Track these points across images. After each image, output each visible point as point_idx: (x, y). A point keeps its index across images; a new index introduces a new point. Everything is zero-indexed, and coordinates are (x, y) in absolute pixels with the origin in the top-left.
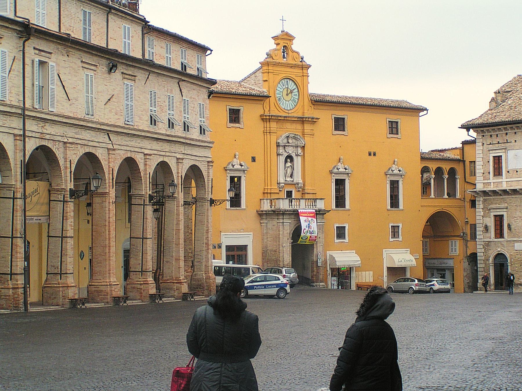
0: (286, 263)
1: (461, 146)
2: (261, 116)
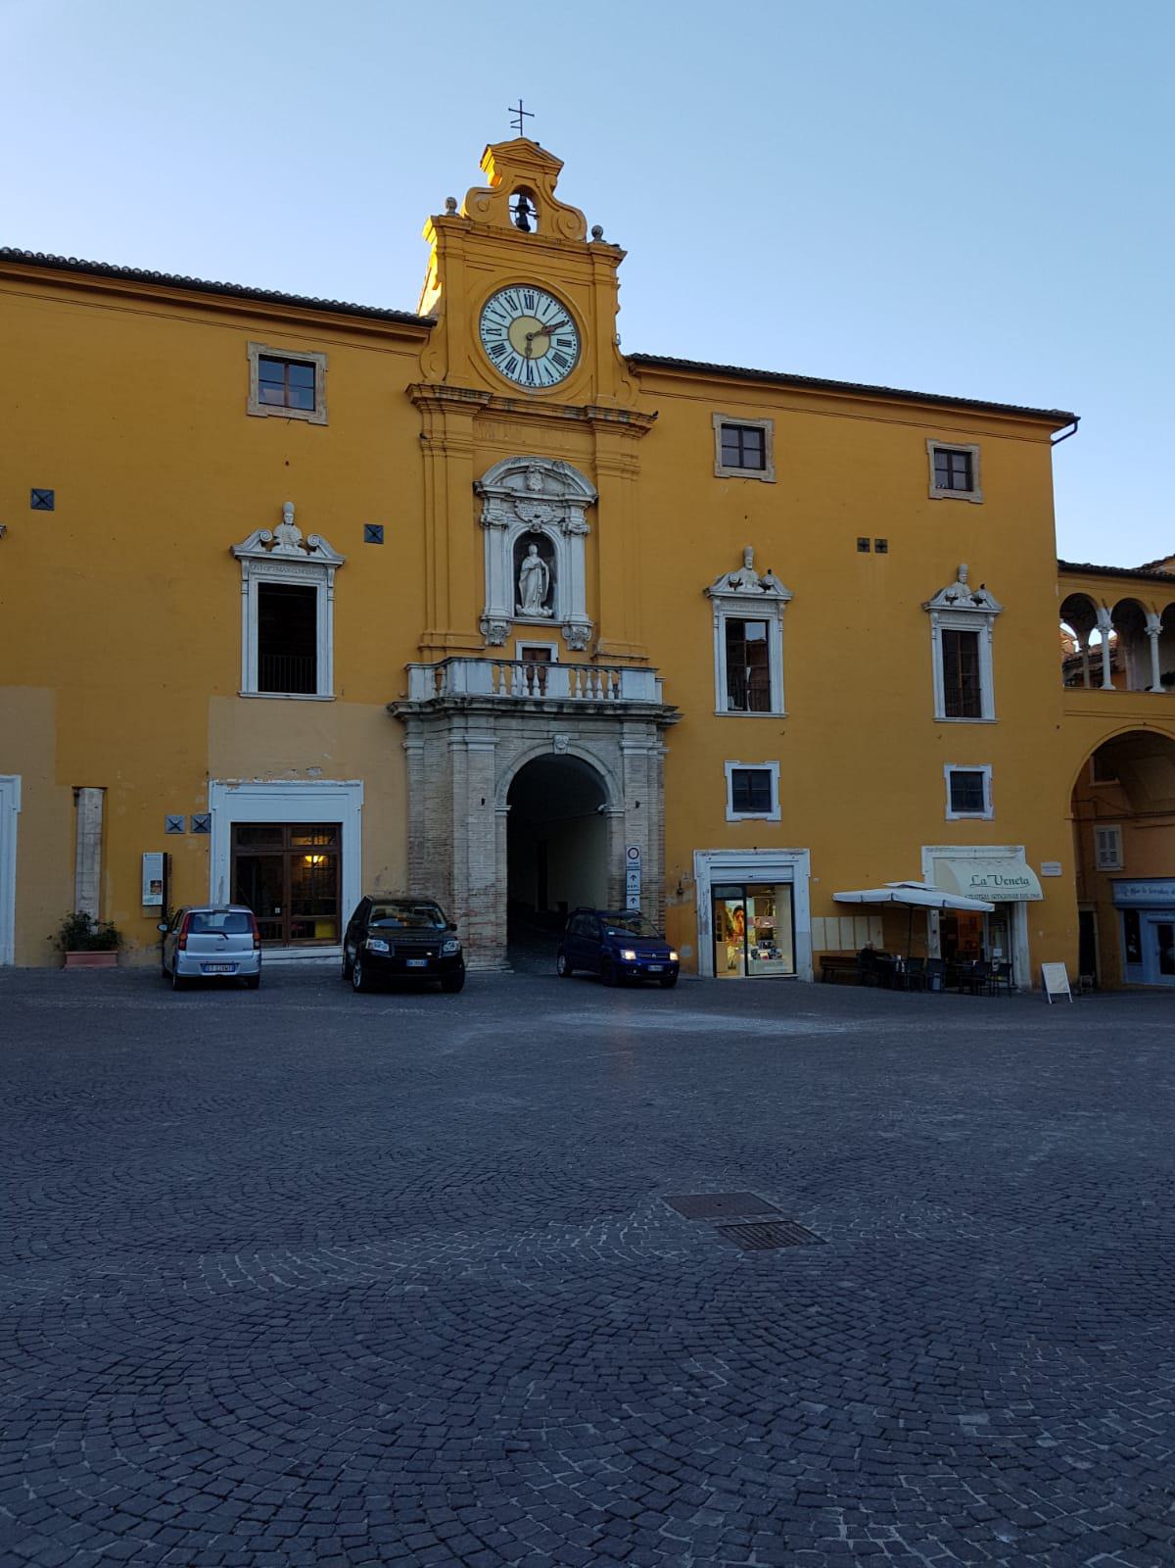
2: (409, 390)
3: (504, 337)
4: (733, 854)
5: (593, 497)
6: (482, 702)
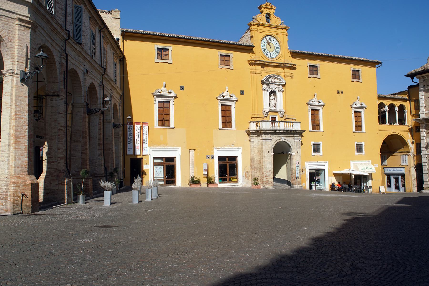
0: (268, 170)
1: (407, 89)
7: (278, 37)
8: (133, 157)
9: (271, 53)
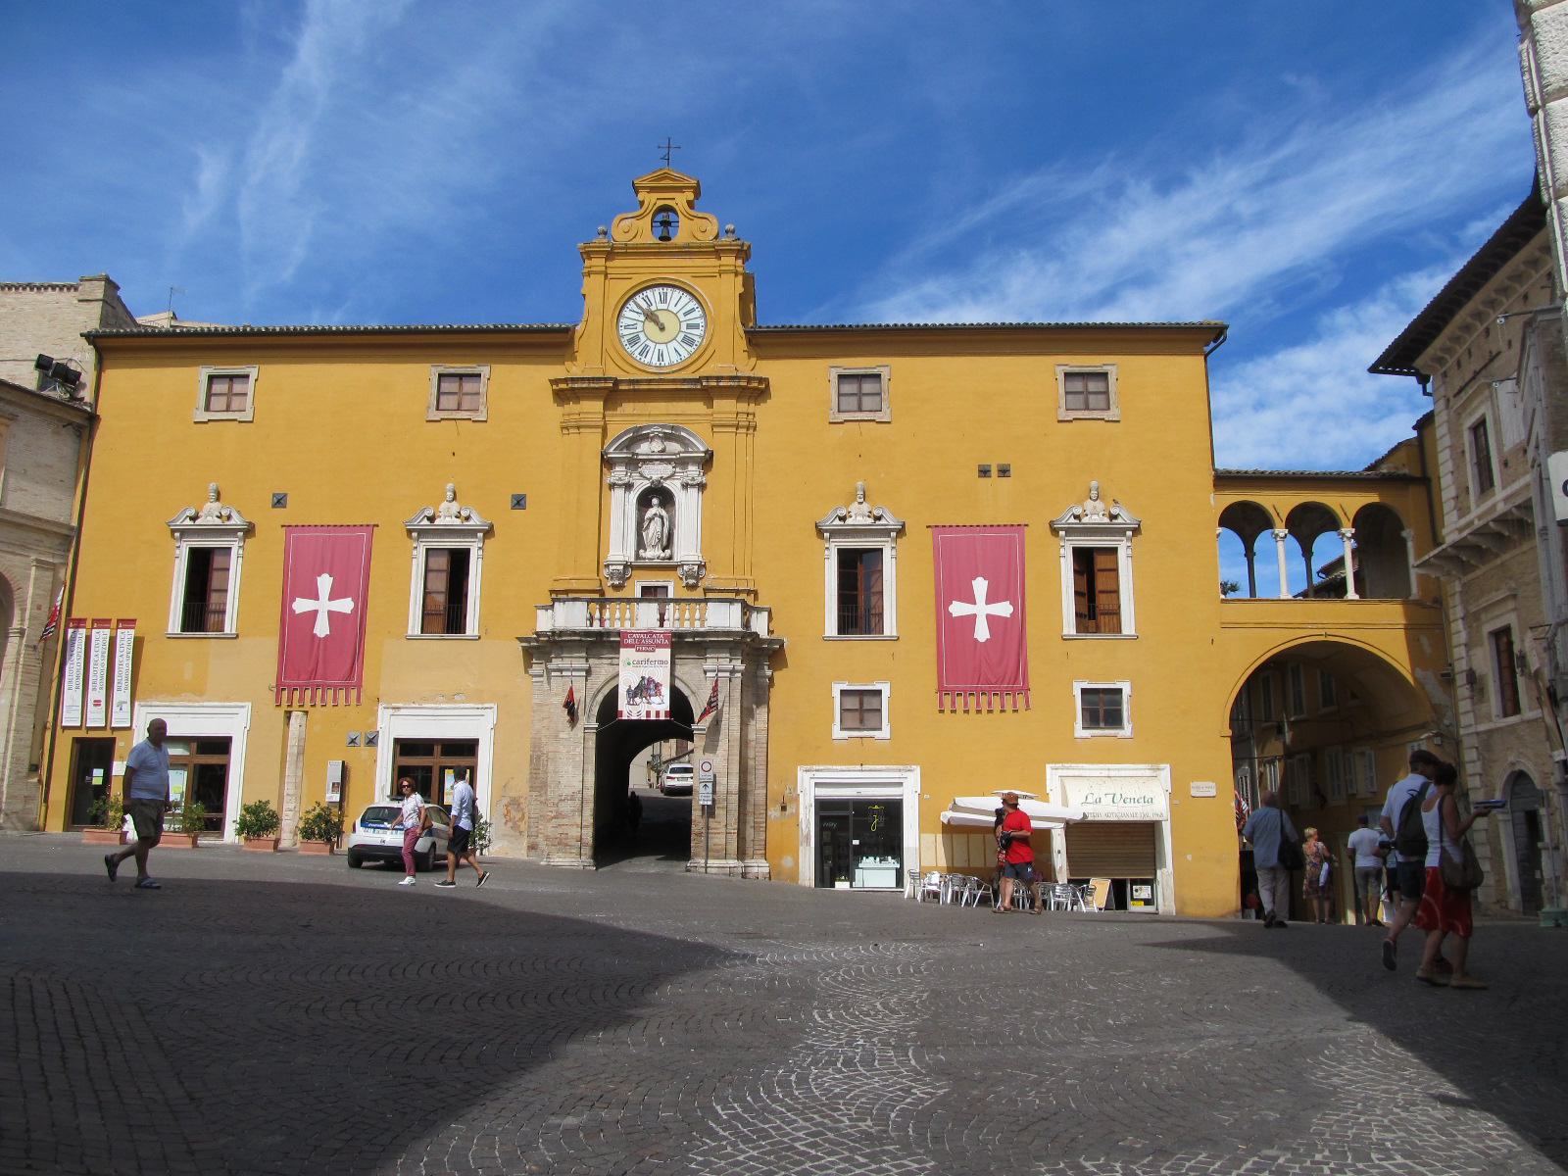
0: (567, 792)
1: (1414, 434)
3: (640, 329)
4: (837, 771)
5: (706, 452)
6: (570, 635)
7: (698, 286)
8: (82, 734)
9: (662, 347)
